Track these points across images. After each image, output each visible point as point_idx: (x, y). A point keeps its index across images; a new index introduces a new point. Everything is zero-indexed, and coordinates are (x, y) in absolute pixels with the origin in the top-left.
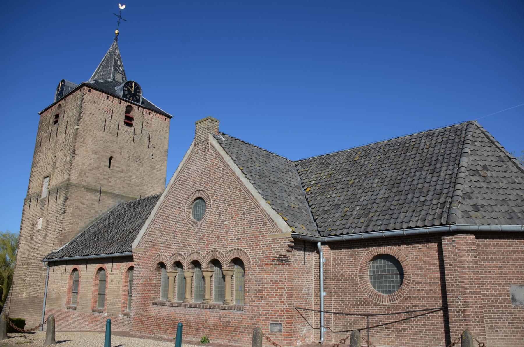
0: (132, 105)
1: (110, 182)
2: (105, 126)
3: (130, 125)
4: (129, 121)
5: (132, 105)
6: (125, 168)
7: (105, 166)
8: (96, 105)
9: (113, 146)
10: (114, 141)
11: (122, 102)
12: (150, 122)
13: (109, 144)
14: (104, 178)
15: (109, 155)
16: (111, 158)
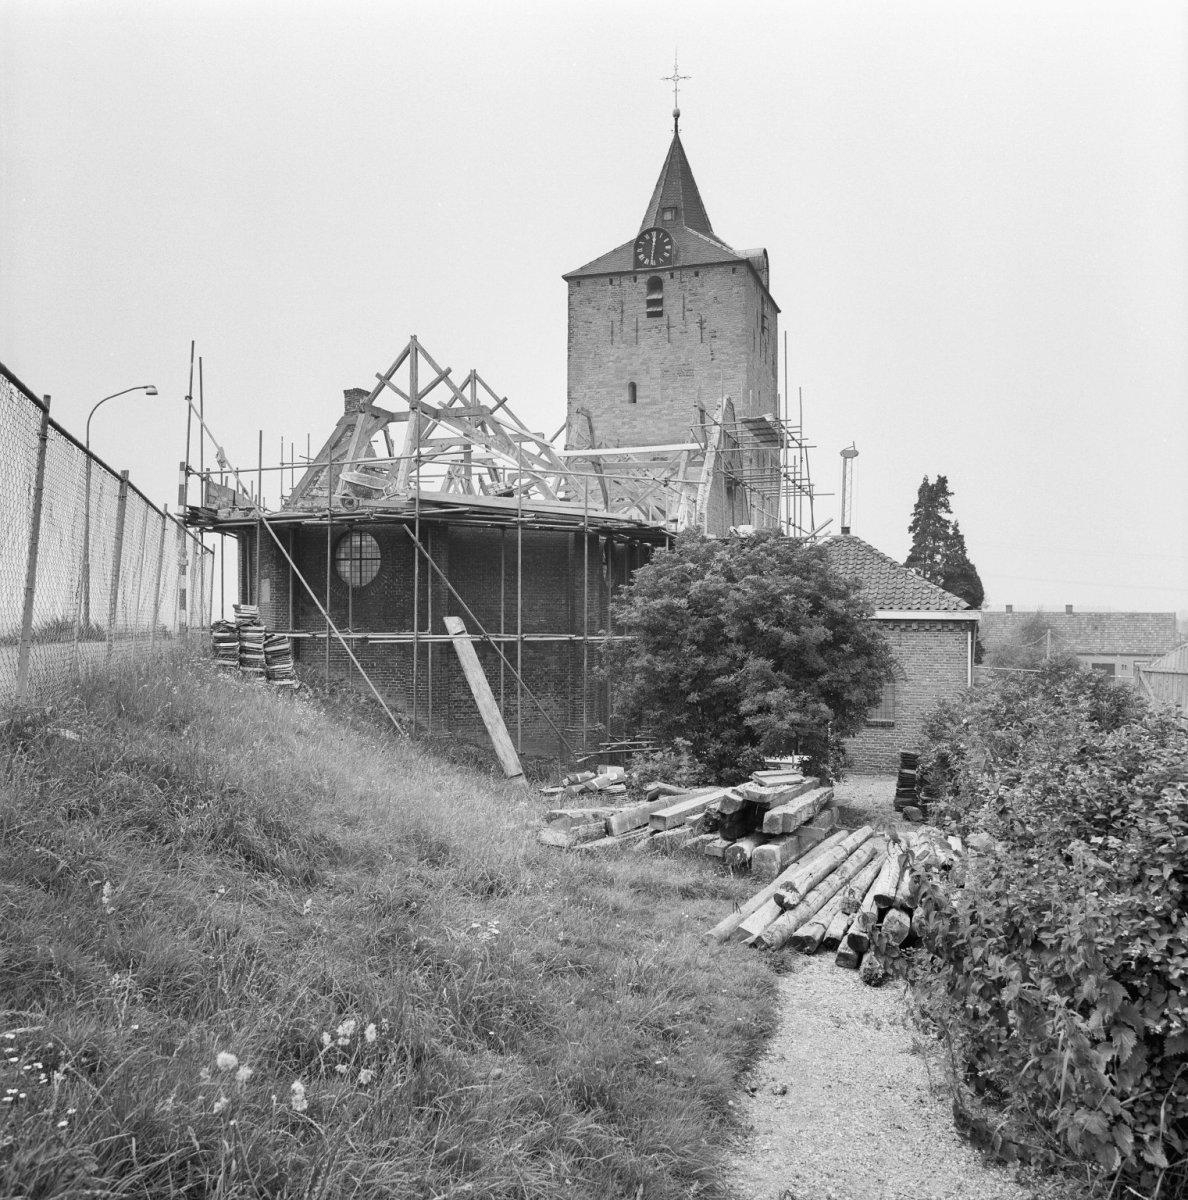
0: (658, 274)
1: (635, 427)
2: (612, 332)
3: (659, 314)
4: (655, 309)
5: (658, 274)
6: (658, 397)
7: (622, 402)
8: (593, 304)
9: (631, 364)
10: (634, 354)
11: (639, 276)
12: (700, 290)
13: (624, 361)
14: (623, 423)
15: (626, 381)
16: (633, 387)
